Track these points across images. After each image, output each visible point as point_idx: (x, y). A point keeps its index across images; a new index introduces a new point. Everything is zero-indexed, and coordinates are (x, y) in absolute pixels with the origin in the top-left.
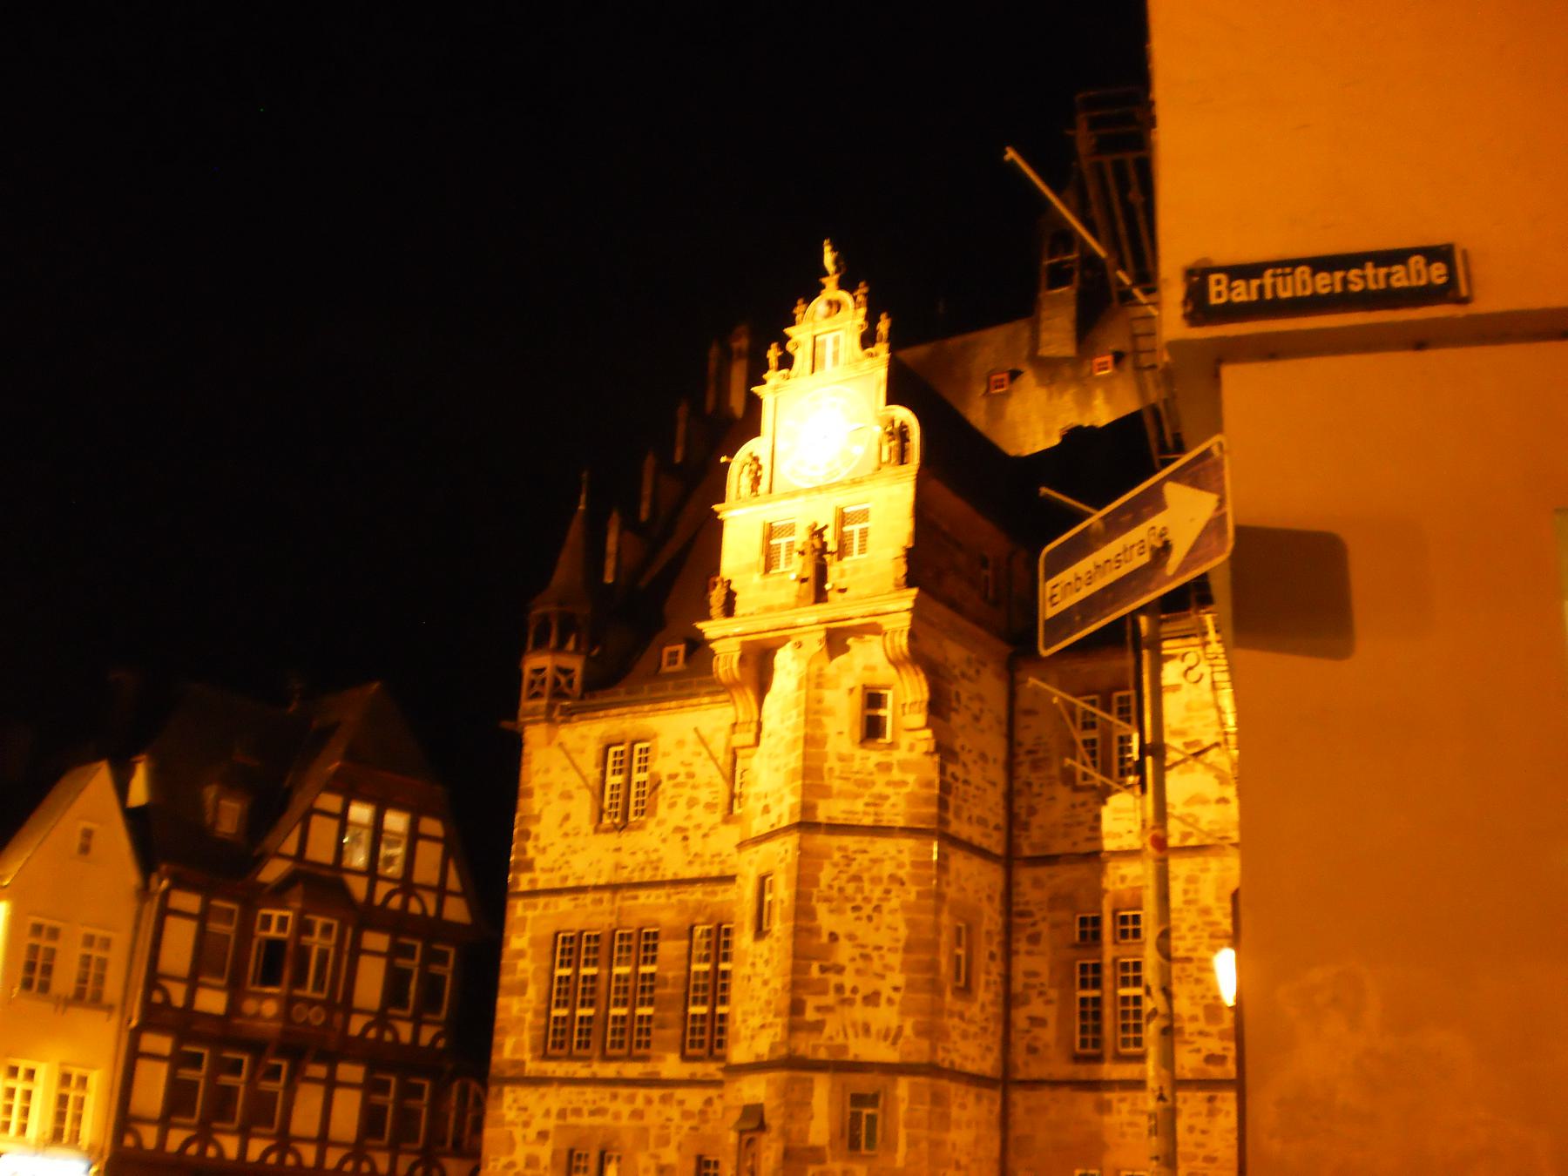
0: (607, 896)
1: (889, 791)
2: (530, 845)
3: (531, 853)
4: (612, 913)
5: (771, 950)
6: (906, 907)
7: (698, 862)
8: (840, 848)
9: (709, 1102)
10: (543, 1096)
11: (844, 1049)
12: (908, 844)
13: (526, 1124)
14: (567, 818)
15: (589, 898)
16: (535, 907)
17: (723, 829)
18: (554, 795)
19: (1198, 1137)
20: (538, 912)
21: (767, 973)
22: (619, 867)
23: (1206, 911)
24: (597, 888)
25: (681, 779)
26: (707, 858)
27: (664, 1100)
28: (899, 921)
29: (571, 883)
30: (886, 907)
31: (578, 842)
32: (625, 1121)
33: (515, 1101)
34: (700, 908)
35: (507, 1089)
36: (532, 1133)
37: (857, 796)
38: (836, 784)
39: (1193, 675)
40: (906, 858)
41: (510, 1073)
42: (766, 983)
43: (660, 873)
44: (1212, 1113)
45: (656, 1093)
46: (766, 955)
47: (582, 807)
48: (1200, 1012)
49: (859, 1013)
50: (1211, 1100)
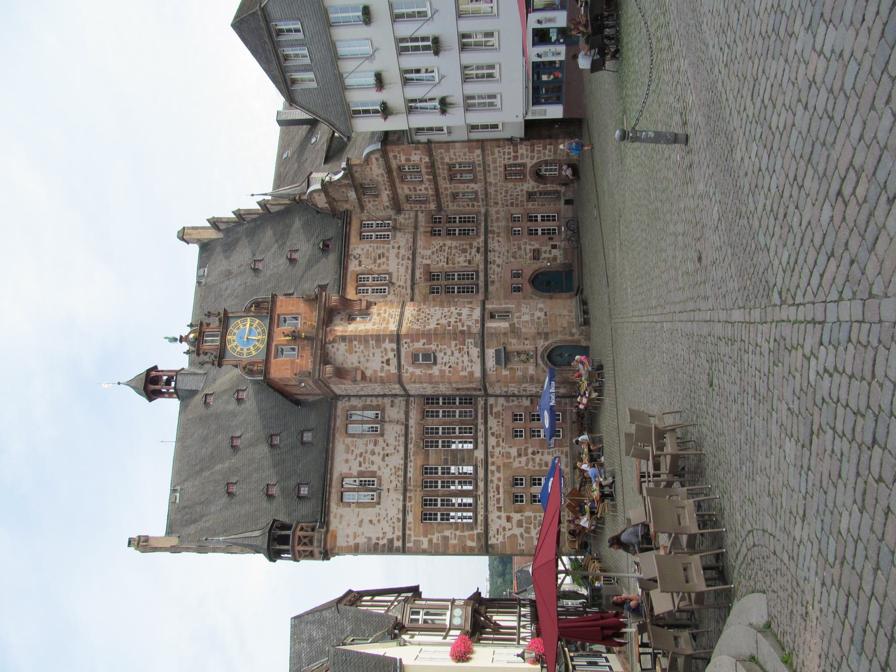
0: (408, 495)
1: (387, 313)
2: (381, 542)
3: (385, 541)
4: (416, 491)
5: (441, 351)
6: (428, 308)
7: (397, 448)
8: (407, 324)
9: (493, 434)
10: (492, 520)
11: (476, 320)
12: (406, 308)
13: (504, 529)
14: (371, 522)
15: (408, 504)
16: (410, 535)
17: (386, 437)
18: (359, 531)
19: (502, 254)
20: (412, 534)
21: (449, 353)
22: (396, 489)
23: (433, 253)
24: (404, 500)
25: (361, 459)
26: (397, 443)
27: (492, 457)
28: (432, 311)
29: (400, 516)
30: (428, 312)
31: (383, 513)
32: (501, 475)
33: (494, 537)
34: (417, 445)
35: (490, 542)
36: (508, 525)
37: (388, 320)
38: (384, 325)
39: (358, 256)
40: (412, 308)
41: (483, 542)
42: (453, 353)
43: (400, 467)
44: (494, 251)
45: (490, 460)
46: (442, 354)
47: (368, 513)
48: (463, 255)
49: (464, 317)
50: (490, 251)
